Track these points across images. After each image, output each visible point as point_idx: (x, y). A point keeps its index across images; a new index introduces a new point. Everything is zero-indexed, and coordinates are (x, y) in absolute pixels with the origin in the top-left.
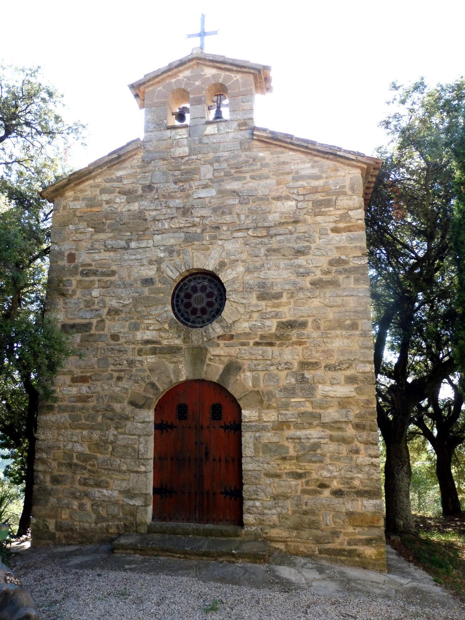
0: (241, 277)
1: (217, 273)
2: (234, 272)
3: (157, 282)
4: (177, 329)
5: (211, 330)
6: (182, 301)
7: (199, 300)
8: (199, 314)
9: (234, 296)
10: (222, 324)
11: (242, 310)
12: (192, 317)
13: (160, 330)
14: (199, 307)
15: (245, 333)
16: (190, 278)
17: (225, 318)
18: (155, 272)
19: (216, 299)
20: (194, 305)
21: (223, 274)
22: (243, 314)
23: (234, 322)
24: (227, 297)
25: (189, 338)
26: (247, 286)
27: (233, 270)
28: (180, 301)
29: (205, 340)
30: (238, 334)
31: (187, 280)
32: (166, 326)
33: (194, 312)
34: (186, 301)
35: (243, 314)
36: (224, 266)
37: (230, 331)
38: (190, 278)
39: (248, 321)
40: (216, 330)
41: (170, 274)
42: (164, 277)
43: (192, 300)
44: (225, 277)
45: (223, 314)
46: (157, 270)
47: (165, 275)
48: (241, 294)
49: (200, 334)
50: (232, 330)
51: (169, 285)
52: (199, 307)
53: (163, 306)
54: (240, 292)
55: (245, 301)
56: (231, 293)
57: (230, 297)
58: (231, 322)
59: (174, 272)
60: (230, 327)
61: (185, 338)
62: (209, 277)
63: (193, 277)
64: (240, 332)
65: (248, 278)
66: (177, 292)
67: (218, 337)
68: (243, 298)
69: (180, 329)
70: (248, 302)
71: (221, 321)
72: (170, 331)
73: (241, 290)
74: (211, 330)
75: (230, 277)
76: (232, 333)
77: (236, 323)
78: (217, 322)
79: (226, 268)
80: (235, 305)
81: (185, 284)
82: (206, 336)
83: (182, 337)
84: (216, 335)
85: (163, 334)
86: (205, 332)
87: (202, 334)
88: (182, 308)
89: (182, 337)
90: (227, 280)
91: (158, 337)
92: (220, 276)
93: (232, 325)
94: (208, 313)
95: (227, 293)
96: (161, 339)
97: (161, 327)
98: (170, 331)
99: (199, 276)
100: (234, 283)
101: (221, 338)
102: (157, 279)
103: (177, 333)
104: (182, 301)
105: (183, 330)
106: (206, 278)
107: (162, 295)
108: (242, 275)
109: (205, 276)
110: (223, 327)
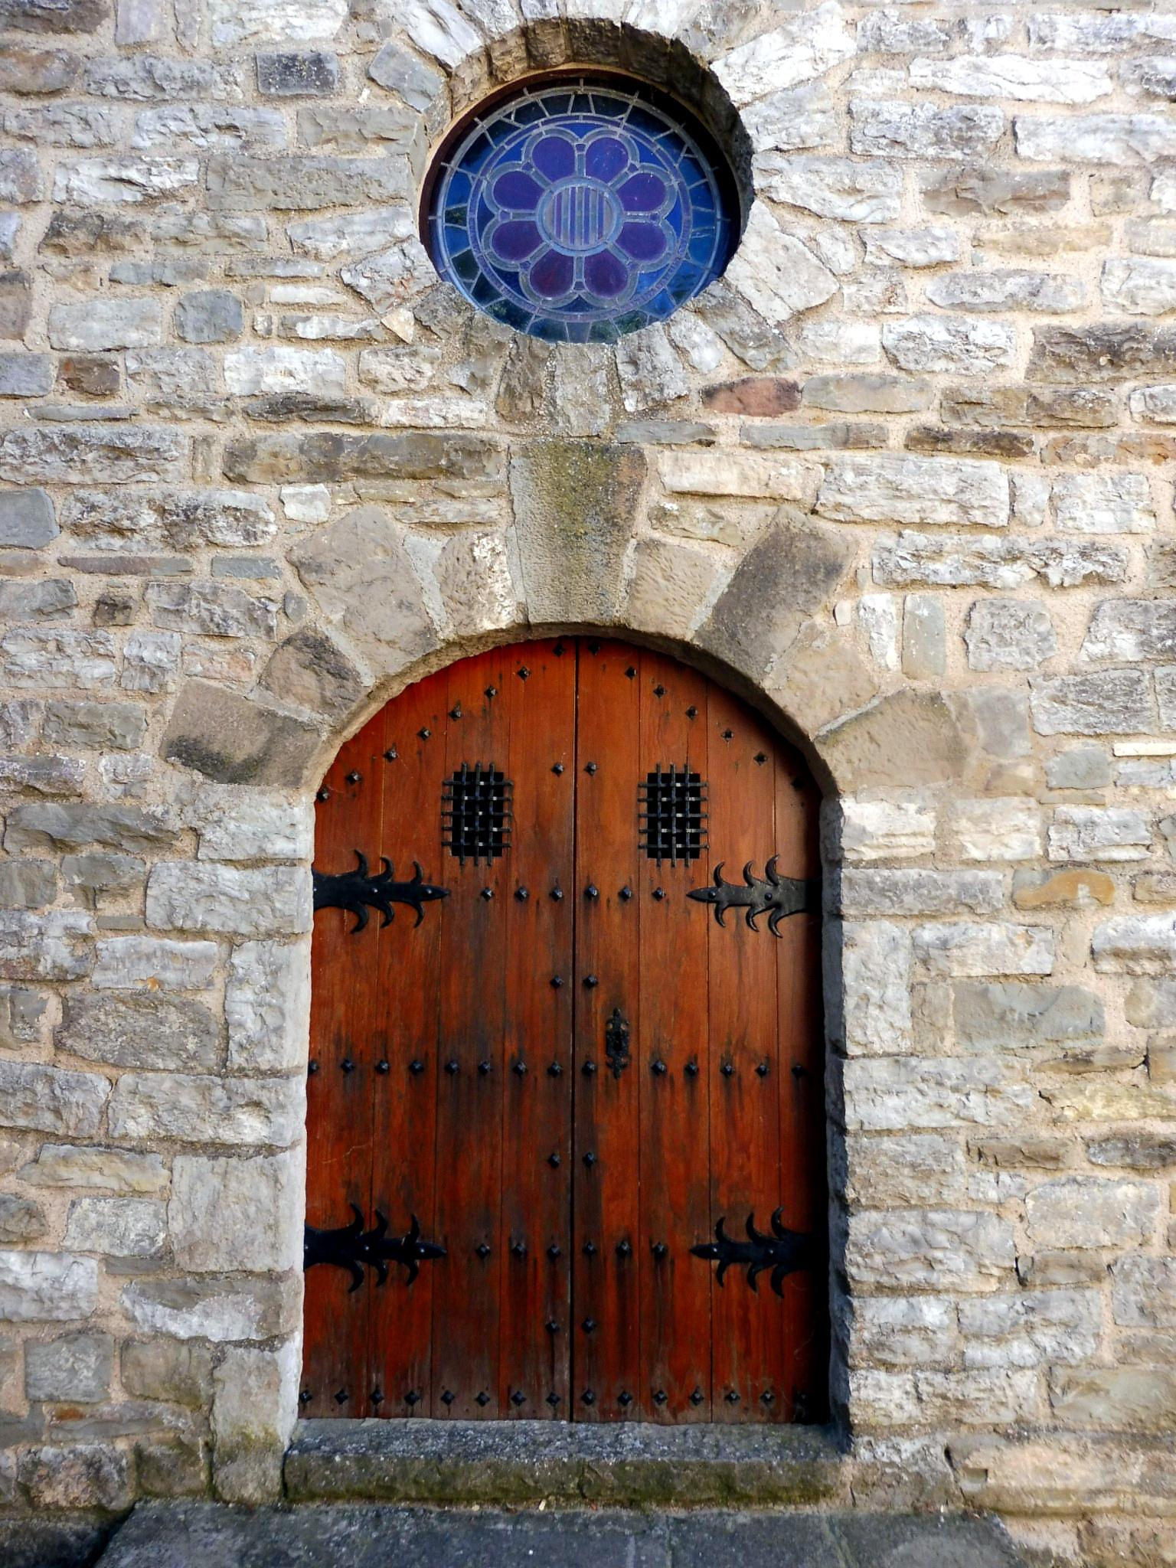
0: (834, 82)
1: (701, 49)
2: (801, 52)
3: (352, 82)
4: (466, 341)
5: (665, 355)
6: (485, 216)
7: (580, 213)
8: (578, 287)
9: (797, 179)
10: (729, 323)
11: (844, 256)
12: (540, 306)
13: (365, 339)
14: (580, 250)
15: (859, 380)
16: (529, 98)
17: (749, 291)
18: (336, 25)
19: (674, 218)
20: (553, 242)
21: (735, 58)
22: (852, 277)
23: (799, 316)
24: (758, 182)
25: (535, 392)
26: (872, 131)
27: (793, 40)
28: (472, 216)
29: (630, 405)
30: (825, 382)
31: (513, 106)
32: (402, 322)
33: (552, 274)
34: (503, 215)
35: (852, 277)
36: (744, 17)
37: (776, 362)
38: (529, 98)
39: (875, 316)
40: (695, 355)
41: (430, 38)
42: (392, 53)
43: (542, 215)
44: (750, 74)
45: (736, 268)
46: (354, 15)
47: (396, 42)
48: (841, 167)
49: (602, 376)
50: (790, 359)
51: (421, 104)
52: (580, 250)
53: (385, 212)
54: (835, 159)
55: (859, 211)
56: (778, 161)
57: (775, 181)
58: (783, 314)
59: (453, 26)
60: (772, 339)
61: (510, 391)
62: (634, 101)
63: (548, 93)
64: (829, 372)
65: (877, 87)
66: (453, 165)
67: (709, 394)
68: (855, 191)
69: (482, 340)
70: (878, 217)
71: (725, 307)
72: (423, 350)
73: (841, 147)
74: (665, 355)
75: (779, 77)
76: (791, 376)
77: (809, 328)
78: (698, 312)
79: (754, 25)
80: (803, 227)
81: (500, 130)
82: (636, 386)
83: (493, 389)
84: (698, 383)
85: (380, 366)
86: (633, 362)
87: (615, 376)
88: (484, 251)
89: (493, 389)
90: (758, 89)
91: (353, 385)
92: (717, 68)
93: (791, 331)
94: (631, 284)
95: (757, 162)
96: (366, 393)
97: (370, 324)
98: (423, 350)
99: (581, 90)
100: (800, 110)
101: (723, 396)
102: (352, 65)
103: (463, 362)
104: (485, 216)
105: (500, 345)
106: (619, 107)
107: (380, 151)
108: (841, 74)
109: (613, 94)
110: (733, 341)
